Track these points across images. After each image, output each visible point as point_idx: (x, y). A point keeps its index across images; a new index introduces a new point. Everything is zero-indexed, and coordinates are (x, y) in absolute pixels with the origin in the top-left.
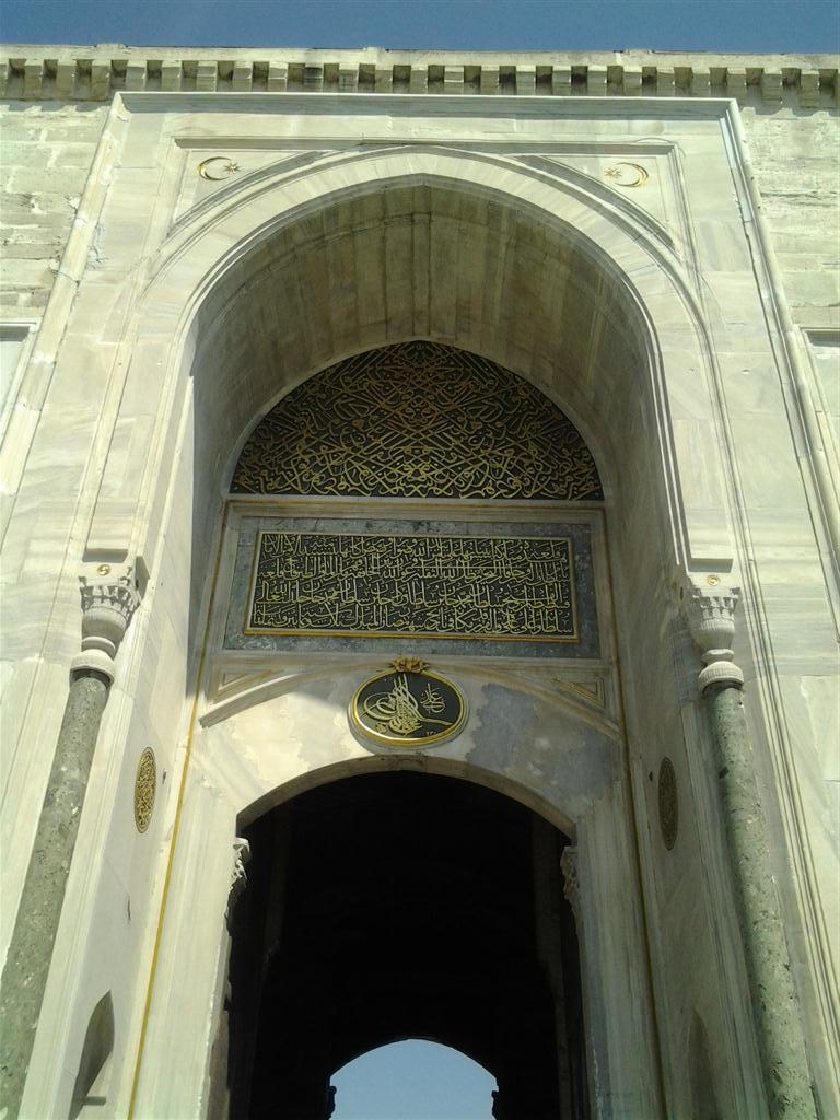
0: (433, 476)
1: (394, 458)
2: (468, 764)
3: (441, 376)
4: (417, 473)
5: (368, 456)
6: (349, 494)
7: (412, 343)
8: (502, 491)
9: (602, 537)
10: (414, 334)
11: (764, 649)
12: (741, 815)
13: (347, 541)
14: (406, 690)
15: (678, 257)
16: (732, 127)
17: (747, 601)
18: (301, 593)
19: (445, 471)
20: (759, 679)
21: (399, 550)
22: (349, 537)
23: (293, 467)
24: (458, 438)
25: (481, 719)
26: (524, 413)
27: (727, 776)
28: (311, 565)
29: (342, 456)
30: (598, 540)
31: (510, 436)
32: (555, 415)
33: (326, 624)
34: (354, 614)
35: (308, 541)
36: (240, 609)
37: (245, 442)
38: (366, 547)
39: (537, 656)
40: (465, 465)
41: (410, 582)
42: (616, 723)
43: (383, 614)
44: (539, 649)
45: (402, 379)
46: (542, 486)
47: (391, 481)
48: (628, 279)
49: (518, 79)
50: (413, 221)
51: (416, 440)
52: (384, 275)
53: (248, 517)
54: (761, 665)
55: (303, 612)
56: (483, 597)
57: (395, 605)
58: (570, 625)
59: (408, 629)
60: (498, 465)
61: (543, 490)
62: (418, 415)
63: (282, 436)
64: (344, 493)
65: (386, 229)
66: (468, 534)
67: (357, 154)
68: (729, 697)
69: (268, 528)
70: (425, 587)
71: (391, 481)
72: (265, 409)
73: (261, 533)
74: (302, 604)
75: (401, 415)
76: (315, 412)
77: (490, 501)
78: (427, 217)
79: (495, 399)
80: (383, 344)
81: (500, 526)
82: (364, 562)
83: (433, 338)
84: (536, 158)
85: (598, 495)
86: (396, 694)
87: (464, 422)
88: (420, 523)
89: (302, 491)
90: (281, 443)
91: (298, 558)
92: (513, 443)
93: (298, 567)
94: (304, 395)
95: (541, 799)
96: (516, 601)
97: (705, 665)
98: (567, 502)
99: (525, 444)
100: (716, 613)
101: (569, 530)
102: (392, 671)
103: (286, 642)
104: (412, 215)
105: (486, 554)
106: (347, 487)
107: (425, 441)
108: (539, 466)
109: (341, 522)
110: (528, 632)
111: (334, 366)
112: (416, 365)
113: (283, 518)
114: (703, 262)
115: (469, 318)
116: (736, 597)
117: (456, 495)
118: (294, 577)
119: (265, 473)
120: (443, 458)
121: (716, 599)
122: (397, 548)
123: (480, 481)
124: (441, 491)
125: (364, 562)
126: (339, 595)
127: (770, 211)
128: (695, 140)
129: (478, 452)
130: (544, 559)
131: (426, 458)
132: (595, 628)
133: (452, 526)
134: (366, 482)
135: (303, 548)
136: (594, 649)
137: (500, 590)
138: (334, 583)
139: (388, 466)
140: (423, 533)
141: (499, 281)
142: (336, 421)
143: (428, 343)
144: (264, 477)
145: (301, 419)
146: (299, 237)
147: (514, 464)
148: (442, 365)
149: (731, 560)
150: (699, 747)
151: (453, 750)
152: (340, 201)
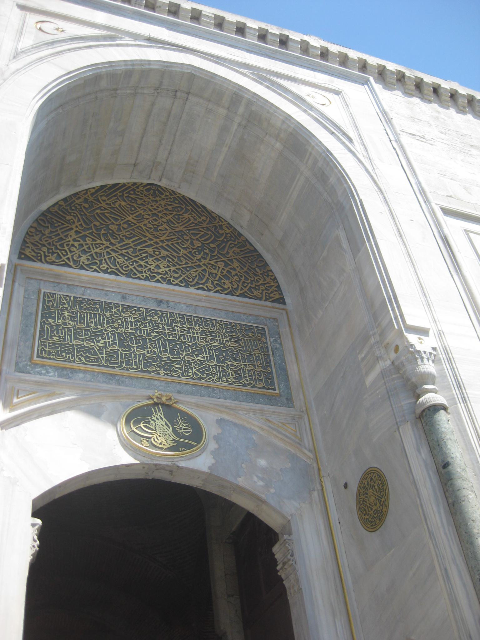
0: (170, 270)
1: (141, 254)
2: (210, 474)
3: (170, 208)
4: (158, 267)
5: (122, 250)
6: (108, 273)
7: (148, 184)
8: (219, 288)
9: (288, 328)
10: (150, 178)
11: (459, 387)
12: (465, 492)
13: (109, 306)
14: (163, 417)
15: (358, 147)
16: (372, 90)
17: (442, 356)
18: (76, 338)
19: (179, 269)
20: (459, 404)
21: (148, 318)
22: (111, 303)
23: (66, 248)
25: (217, 443)
26: (228, 241)
27: (450, 467)
28: (82, 319)
29: (103, 247)
30: (284, 330)
31: (221, 254)
32: (248, 246)
33: (96, 362)
34: (117, 358)
35: (79, 301)
36: (27, 343)
37: (29, 226)
38: (124, 312)
39: (252, 402)
40: (192, 267)
41: (158, 340)
42: (310, 451)
43: (140, 361)
44: (253, 397)
46: (245, 290)
47: (140, 269)
48: (331, 154)
49: (247, 30)
50: (175, 95)
51: (156, 246)
52: (145, 130)
53: (31, 278)
54: (459, 396)
55: (78, 352)
56: (212, 357)
57: (148, 355)
58: (272, 383)
59: (159, 374)
60: (214, 271)
61: (246, 292)
63: (57, 227)
64: (106, 272)
65: (157, 96)
66: (196, 313)
67: (145, 44)
68: (442, 416)
69: (46, 289)
70: (169, 345)
71: (140, 269)
72: (44, 207)
73: (43, 291)
74: (76, 345)
75: (144, 228)
76: (81, 215)
77: (211, 294)
78: (186, 95)
79: (208, 229)
80: (125, 181)
81: (218, 311)
82: (122, 322)
83: (164, 183)
84: (261, 76)
85: (282, 301)
86: (155, 419)
87: (188, 240)
88: (161, 301)
89: (73, 266)
90: (57, 231)
91: (72, 312)
92: (223, 259)
93: (73, 318)
94: (72, 203)
95: (264, 502)
96: (235, 363)
97: (419, 397)
98: (262, 302)
99: (231, 260)
100: (425, 360)
101: (264, 321)
102: (151, 402)
103: (65, 372)
104: (176, 91)
105: (211, 328)
106: (107, 268)
107: (162, 247)
108: (242, 276)
109: (104, 292)
110: (245, 385)
111: (93, 188)
112: (151, 198)
113: (59, 283)
114: (373, 155)
115: (194, 173)
116: (434, 353)
117: (187, 286)
118: (69, 326)
120: (176, 260)
121: (425, 352)
122: (147, 316)
123: (202, 279)
124: (176, 282)
125: (122, 322)
126: (105, 343)
127: (404, 139)
128: (353, 91)
129: (199, 260)
130: (251, 337)
131: (164, 258)
132: (288, 387)
133: (184, 307)
134: (121, 267)
135: (75, 306)
136: (289, 402)
139: (136, 259)
140: (163, 308)
141: (225, 149)
142: (97, 224)
143: (160, 186)
144: (44, 252)
145: (72, 217)
146: (104, 84)
147: (225, 272)
148: (170, 201)
149: (430, 329)
150: (419, 451)
151: (199, 465)
152: (136, 67)
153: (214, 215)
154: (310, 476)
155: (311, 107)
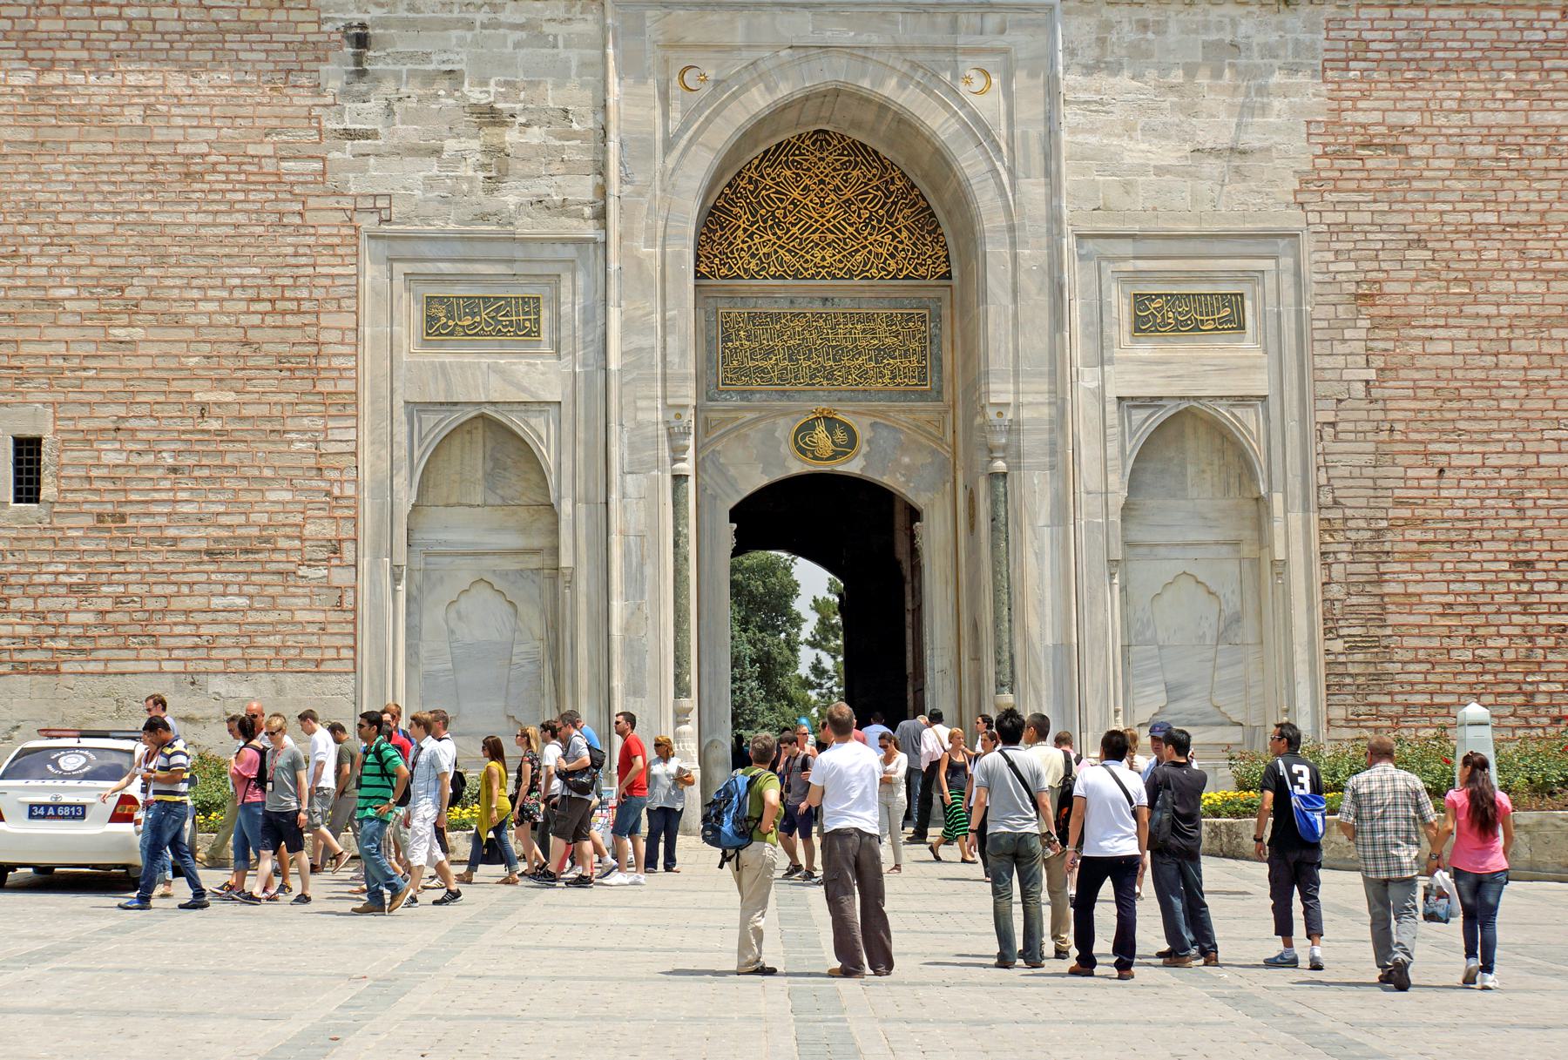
4: (823, 259)
24: (851, 225)
45: (809, 169)
58: (925, 379)
62: (822, 206)
64: (774, 277)
77: (875, 282)
79: (878, 189)
93: (748, 338)
99: (899, 231)
117: (851, 278)
119: (717, 261)
137: (881, 352)
138: (771, 351)
143: (826, 132)
151: (852, 466)
153: (886, 163)
154: (947, 468)
155: (963, 104)
